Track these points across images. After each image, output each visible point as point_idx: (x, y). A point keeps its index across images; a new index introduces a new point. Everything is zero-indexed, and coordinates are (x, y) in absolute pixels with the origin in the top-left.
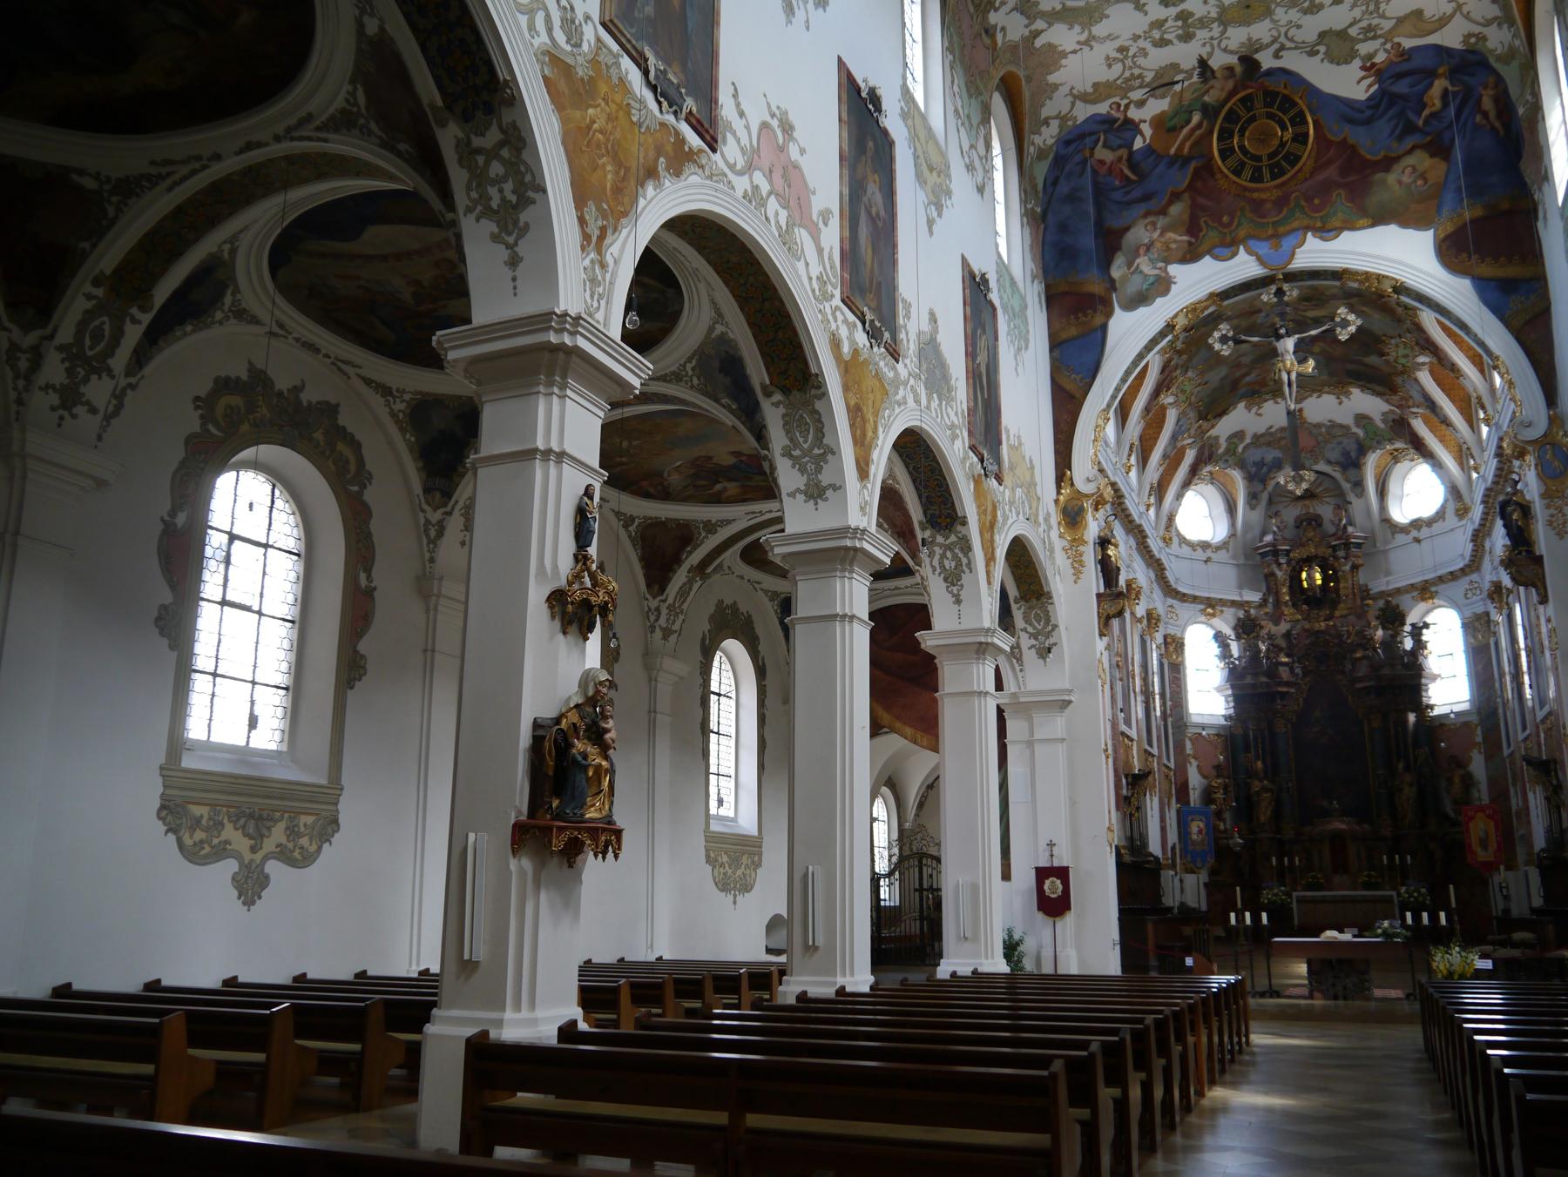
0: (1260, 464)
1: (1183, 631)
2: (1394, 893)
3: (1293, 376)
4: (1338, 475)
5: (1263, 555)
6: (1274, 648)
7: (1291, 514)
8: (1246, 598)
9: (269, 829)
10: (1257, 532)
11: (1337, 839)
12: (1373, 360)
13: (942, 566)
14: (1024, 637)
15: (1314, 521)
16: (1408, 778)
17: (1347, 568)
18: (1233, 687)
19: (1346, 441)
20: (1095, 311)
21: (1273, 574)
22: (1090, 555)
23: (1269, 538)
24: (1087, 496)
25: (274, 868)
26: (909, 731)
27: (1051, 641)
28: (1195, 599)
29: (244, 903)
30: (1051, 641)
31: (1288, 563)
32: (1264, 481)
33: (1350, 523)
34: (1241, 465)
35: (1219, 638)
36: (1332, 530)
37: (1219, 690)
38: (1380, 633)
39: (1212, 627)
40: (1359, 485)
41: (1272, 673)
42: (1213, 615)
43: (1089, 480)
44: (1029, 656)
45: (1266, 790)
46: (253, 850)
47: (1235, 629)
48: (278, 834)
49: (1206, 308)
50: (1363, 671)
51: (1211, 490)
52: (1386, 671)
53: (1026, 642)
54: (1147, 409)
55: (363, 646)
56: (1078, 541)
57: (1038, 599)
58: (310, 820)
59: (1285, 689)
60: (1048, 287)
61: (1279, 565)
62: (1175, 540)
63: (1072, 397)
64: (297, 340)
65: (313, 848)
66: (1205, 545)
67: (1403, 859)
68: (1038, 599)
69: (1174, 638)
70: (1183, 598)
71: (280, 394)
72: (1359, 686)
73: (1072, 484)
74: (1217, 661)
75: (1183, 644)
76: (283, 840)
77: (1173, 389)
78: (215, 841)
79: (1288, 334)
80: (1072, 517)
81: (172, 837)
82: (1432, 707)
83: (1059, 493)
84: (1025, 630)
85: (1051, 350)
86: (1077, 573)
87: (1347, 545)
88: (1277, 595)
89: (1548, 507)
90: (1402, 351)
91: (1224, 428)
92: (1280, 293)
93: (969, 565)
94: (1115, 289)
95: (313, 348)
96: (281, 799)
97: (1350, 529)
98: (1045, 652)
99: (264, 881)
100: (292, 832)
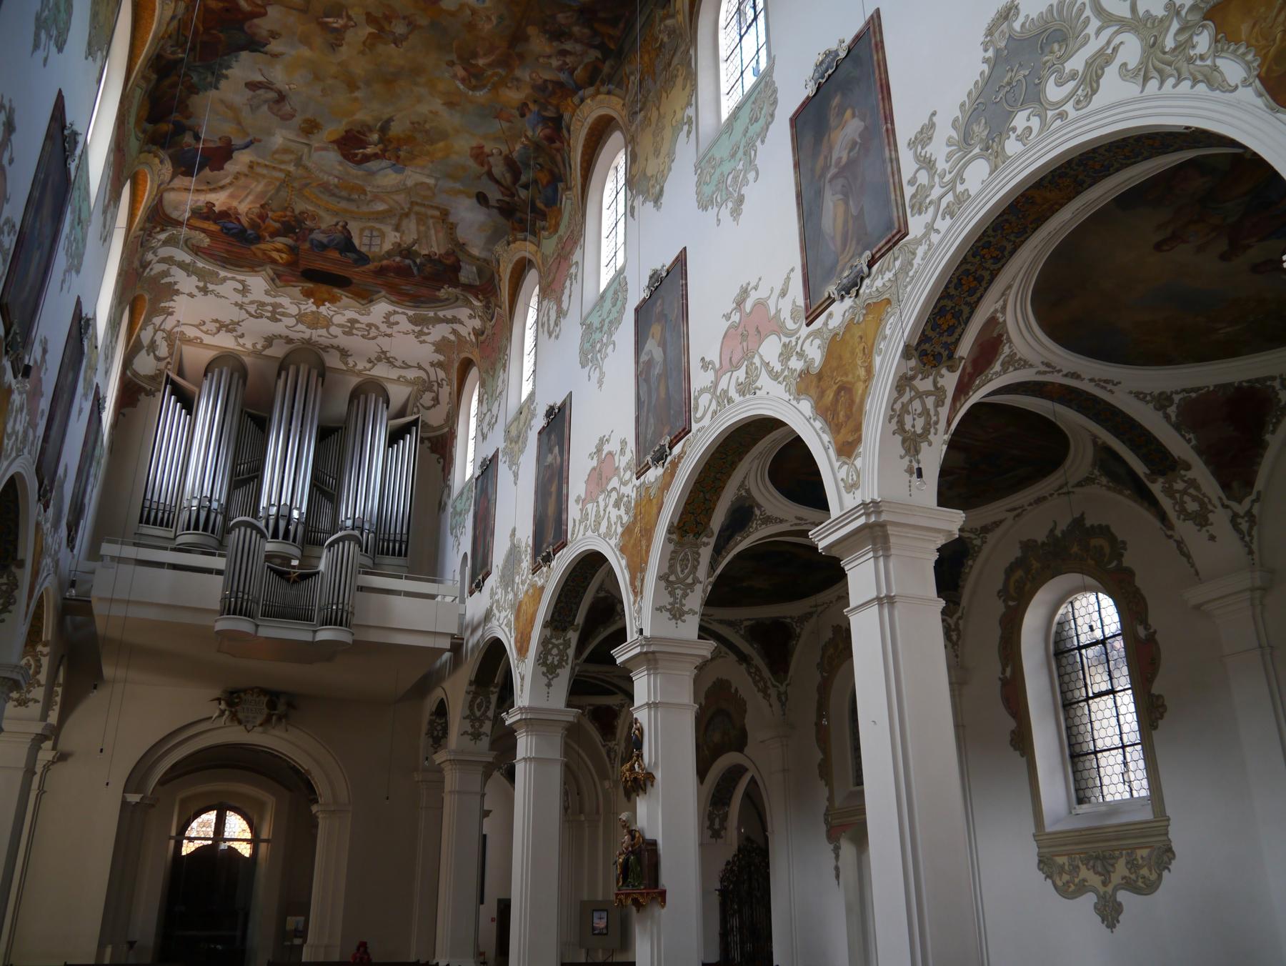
9: (1113, 865)
25: (1123, 896)
29: (1108, 926)
46: (1104, 884)
48: (1121, 869)
55: (1156, 689)
58: (1145, 852)
64: (1030, 504)
65: (1154, 877)
71: (1043, 544)
76: (1127, 873)
78: (1077, 880)
81: (1049, 881)
95: (1039, 500)
96: (1118, 839)
99: (1118, 908)
100: (1133, 865)
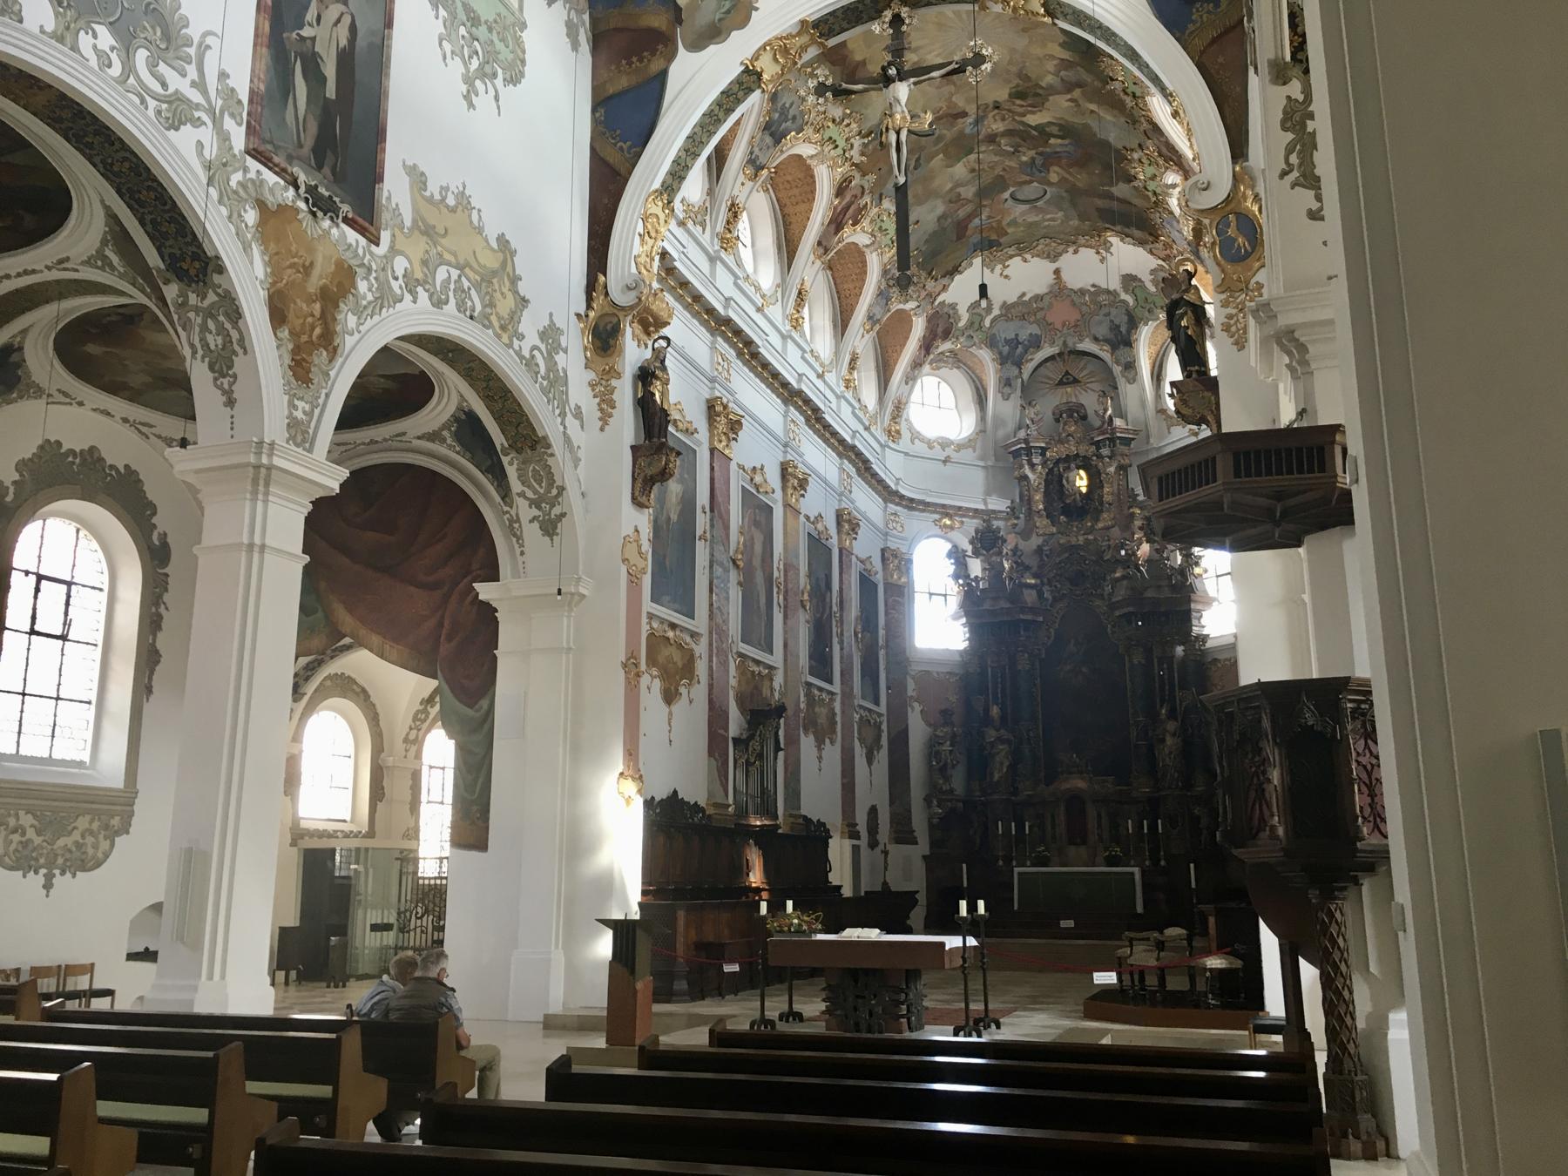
0: (1014, 343)
1: (911, 546)
2: (1136, 870)
3: (903, 137)
4: (1106, 356)
5: (1016, 454)
6: (1020, 566)
7: (1050, 402)
8: (991, 507)
10: (1011, 427)
11: (1075, 802)
12: (1121, 190)
13: (205, 345)
14: (522, 504)
15: (1076, 413)
16: (1171, 726)
17: (1112, 469)
18: (967, 614)
19: (1114, 311)
20: (653, 54)
21: (1026, 478)
22: (625, 392)
23: (1022, 434)
24: (623, 308)
26: (375, 639)
27: (556, 511)
28: (925, 506)
30: (556, 511)
31: (1044, 464)
32: (1019, 365)
33: (1120, 413)
34: (991, 343)
35: (957, 556)
36: (1097, 423)
37: (956, 617)
38: (1145, 549)
39: (949, 540)
40: (1130, 366)
41: (1015, 598)
42: (951, 528)
43: (629, 289)
44: (531, 532)
45: (1000, 740)
47: (971, 542)
49: (804, 49)
50: (1121, 593)
51: (957, 375)
52: (1149, 594)
53: (525, 511)
54: (822, 245)
56: (613, 373)
57: (533, 448)
59: (1029, 617)
60: (594, 22)
61: (1032, 466)
62: (906, 435)
63: (616, 173)
66: (944, 443)
67: (1153, 827)
68: (533, 448)
69: (896, 554)
70: (911, 504)
72: (1117, 613)
73: (607, 294)
74: (951, 582)
75: (910, 561)
77: (865, 223)
79: (902, 77)
80: (604, 339)
82: (1205, 638)
83: (589, 307)
84: (522, 495)
85: (594, 110)
86: (605, 418)
87: (1112, 440)
88: (1029, 501)
89: (1225, 304)
90: (1150, 170)
91: (960, 291)
92: (897, 20)
93: (241, 341)
94: (679, 21)
97: (1118, 422)
98: (550, 528)
